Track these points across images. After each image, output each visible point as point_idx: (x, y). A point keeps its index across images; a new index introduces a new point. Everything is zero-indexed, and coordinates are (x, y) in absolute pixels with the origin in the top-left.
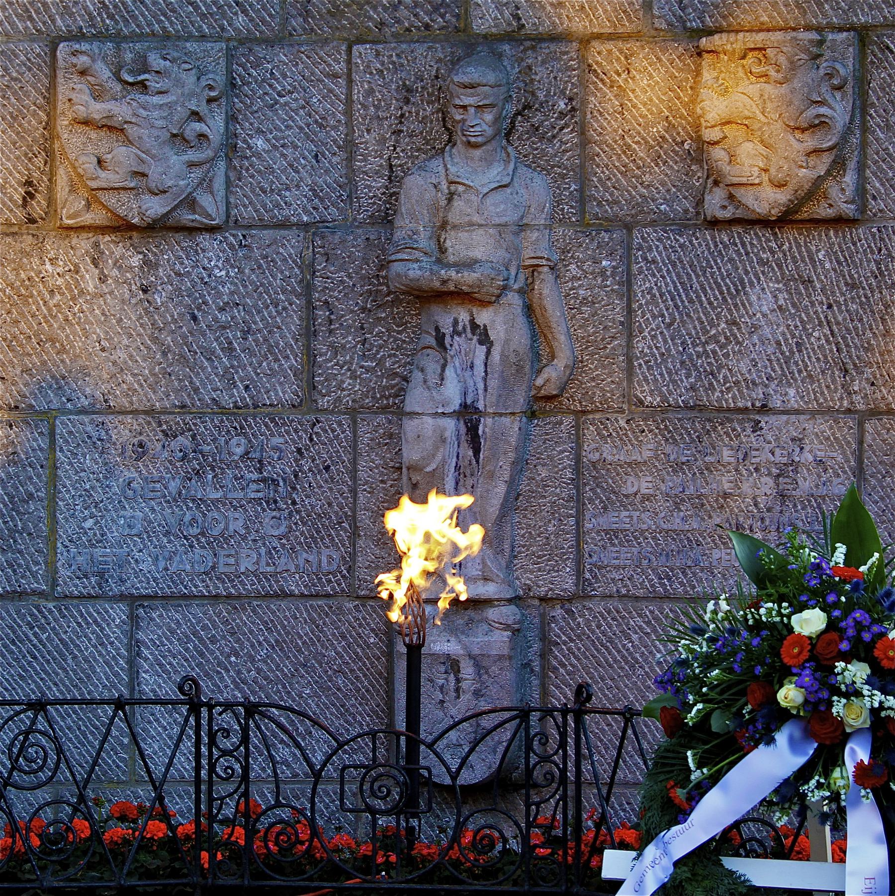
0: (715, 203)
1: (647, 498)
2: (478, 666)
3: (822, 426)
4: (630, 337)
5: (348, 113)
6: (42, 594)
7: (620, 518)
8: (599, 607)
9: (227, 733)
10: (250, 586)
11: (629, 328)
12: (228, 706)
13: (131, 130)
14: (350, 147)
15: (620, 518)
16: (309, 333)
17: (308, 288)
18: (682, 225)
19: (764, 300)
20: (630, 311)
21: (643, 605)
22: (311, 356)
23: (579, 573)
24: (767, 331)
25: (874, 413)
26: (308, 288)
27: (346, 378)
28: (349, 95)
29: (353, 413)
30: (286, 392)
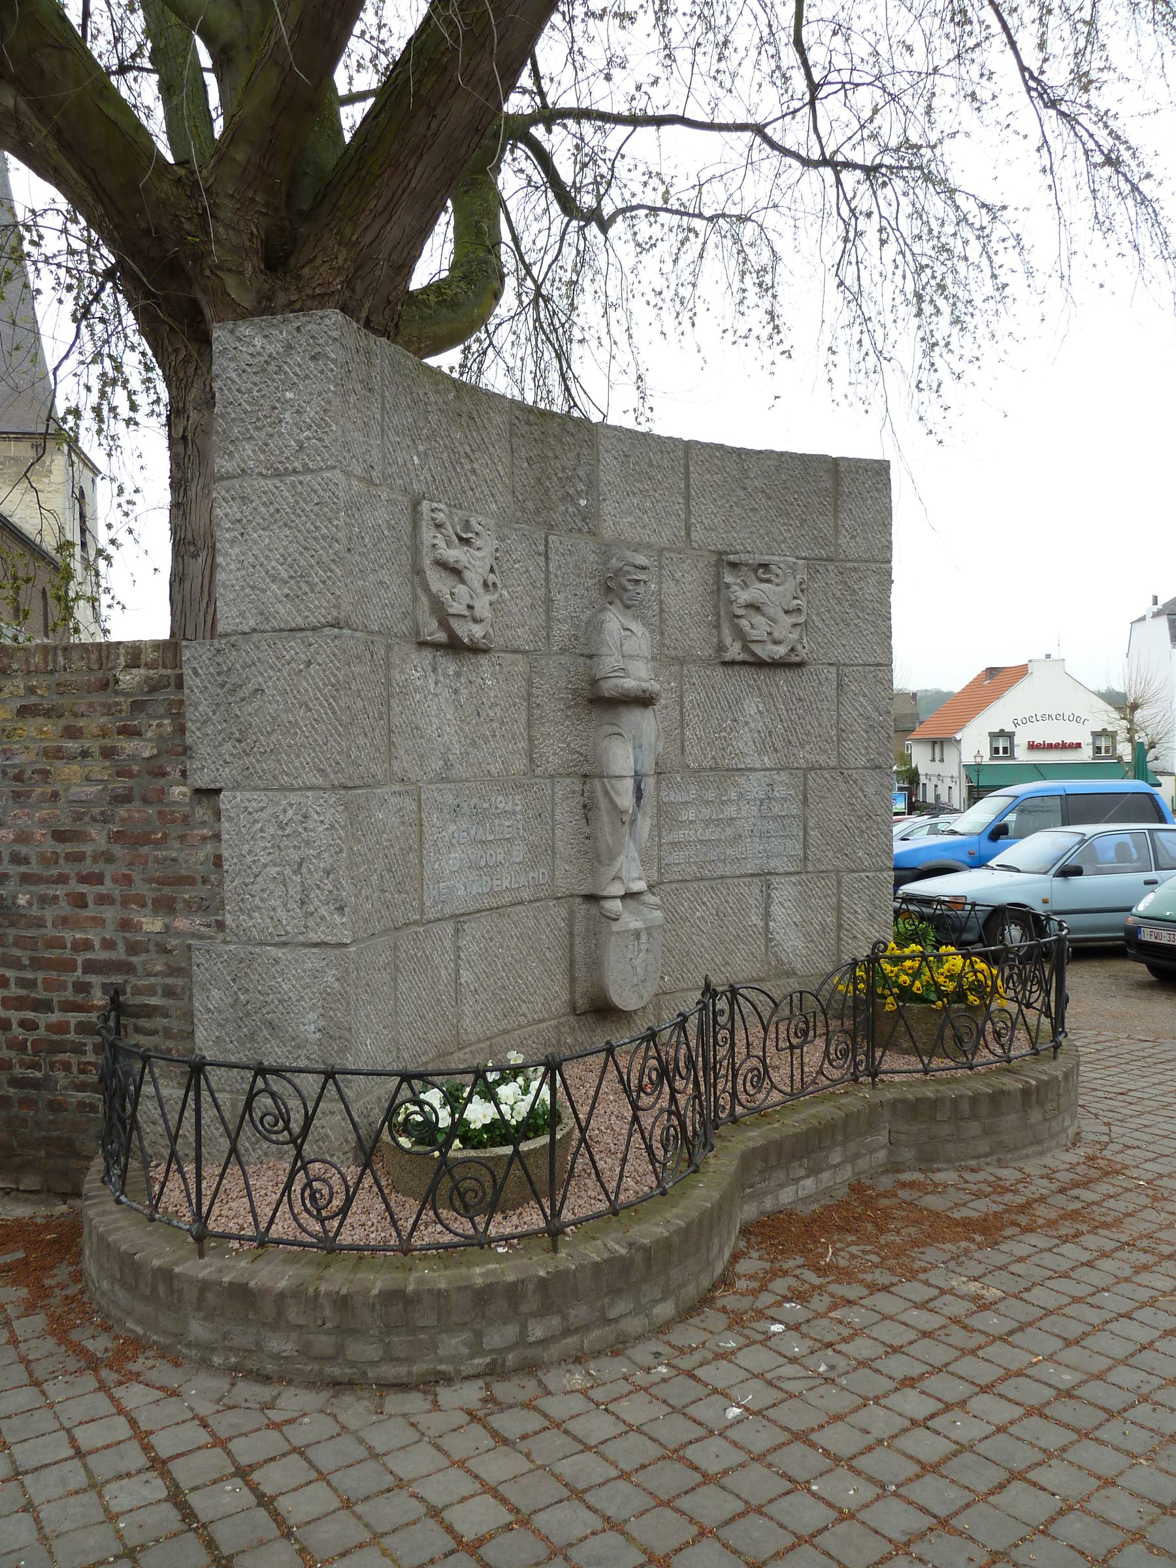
0: (734, 651)
1: (691, 822)
2: (649, 934)
3: (784, 776)
4: (683, 728)
5: (547, 579)
6: (416, 923)
7: (679, 835)
8: (667, 887)
9: (722, 1011)
10: (507, 898)
11: (683, 724)
12: (723, 993)
13: (467, 575)
14: (549, 602)
15: (679, 835)
16: (529, 726)
17: (530, 695)
18: (706, 663)
19: (751, 706)
20: (682, 713)
21: (688, 884)
22: (531, 740)
23: (659, 870)
24: (753, 725)
25: (812, 769)
26: (530, 695)
27: (553, 754)
28: (547, 567)
29: (552, 776)
30: (519, 764)
